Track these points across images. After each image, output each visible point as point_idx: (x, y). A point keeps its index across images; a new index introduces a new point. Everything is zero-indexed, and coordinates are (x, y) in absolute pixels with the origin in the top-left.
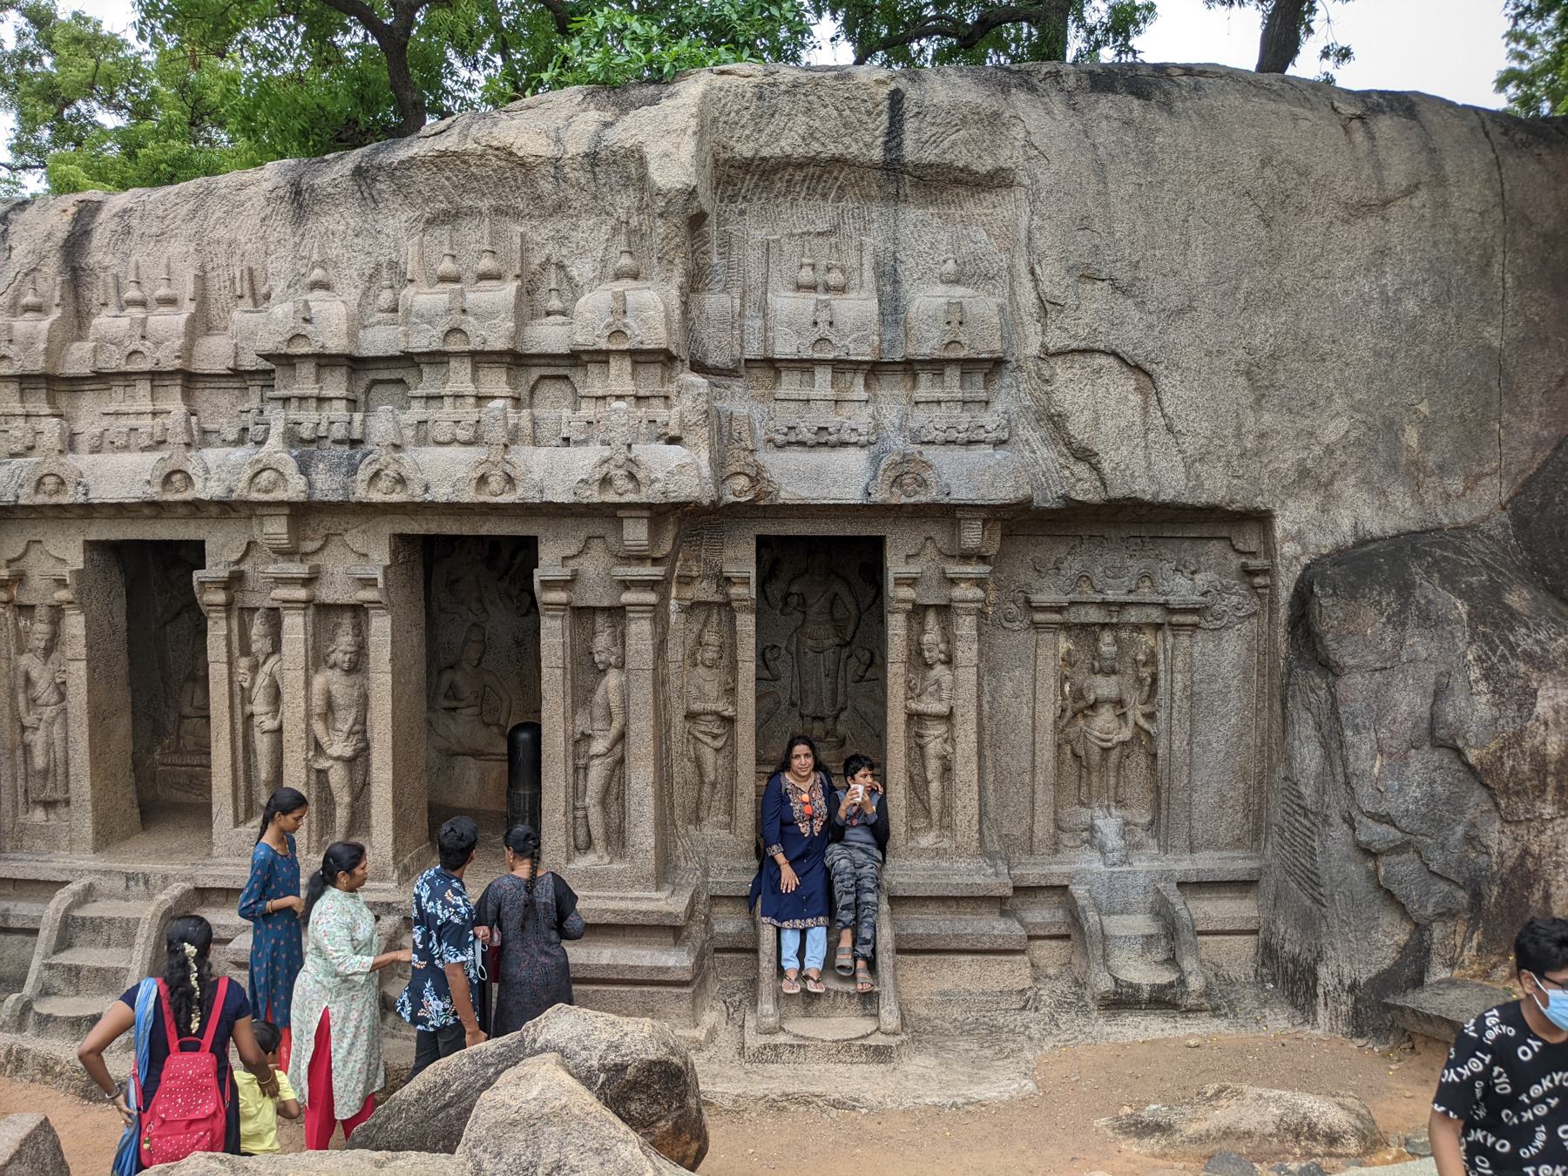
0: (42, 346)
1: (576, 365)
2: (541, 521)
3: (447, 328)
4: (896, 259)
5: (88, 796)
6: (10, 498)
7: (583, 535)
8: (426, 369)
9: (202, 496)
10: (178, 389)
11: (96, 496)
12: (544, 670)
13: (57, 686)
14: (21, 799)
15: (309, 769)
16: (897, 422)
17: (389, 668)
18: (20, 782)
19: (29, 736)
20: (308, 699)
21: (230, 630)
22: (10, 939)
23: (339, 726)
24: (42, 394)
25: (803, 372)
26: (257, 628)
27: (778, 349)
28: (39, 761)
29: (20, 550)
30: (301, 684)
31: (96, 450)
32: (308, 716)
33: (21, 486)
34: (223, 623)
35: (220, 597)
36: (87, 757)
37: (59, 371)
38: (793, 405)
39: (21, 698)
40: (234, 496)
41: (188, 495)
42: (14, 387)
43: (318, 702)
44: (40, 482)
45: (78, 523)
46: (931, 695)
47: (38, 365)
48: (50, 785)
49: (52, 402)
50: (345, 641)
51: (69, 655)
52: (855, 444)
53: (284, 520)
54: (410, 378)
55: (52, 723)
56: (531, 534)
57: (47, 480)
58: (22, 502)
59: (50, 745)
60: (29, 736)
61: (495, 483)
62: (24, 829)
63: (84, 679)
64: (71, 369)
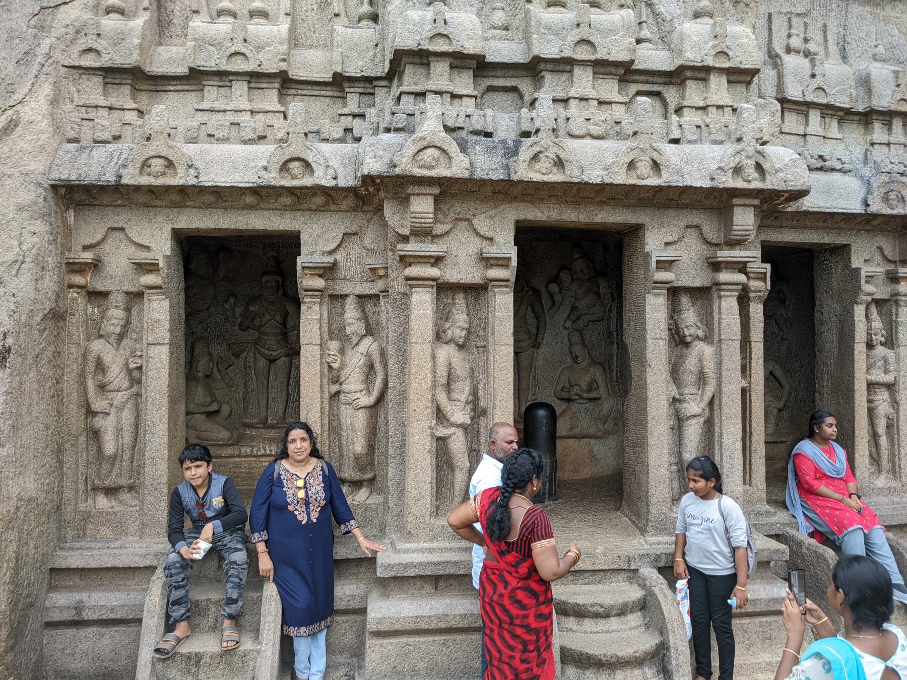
0: (136, 41)
1: (670, 83)
2: (648, 211)
3: (577, 38)
4: (845, 40)
5: (165, 479)
6: (111, 178)
7: (683, 224)
8: (548, 76)
9: (324, 183)
10: (275, 92)
11: (209, 179)
12: (649, 341)
13: (129, 372)
14: (81, 487)
15: (433, 435)
16: (861, 157)
17: (511, 341)
18: (81, 468)
19: (99, 422)
20: (434, 370)
21: (322, 316)
22: (83, 632)
23: (455, 395)
24: (126, 90)
25: (799, 112)
26: (351, 312)
27: (790, 92)
28: (109, 447)
29: (99, 237)
30: (429, 356)
31: (194, 140)
32: (434, 387)
33: (125, 166)
34: (316, 308)
35: (319, 283)
36: (165, 439)
37: (147, 69)
38: (793, 138)
39: (91, 384)
40: (398, 171)
41: (307, 181)
42: (97, 80)
43: (442, 373)
44: (145, 164)
45: (166, 211)
46: (880, 368)
47: (130, 59)
48: (114, 473)
49: (134, 98)
50: (460, 317)
51: (151, 340)
52: (840, 170)
53: (431, 200)
54: (525, 86)
55: (121, 409)
56: (640, 221)
57: (154, 162)
58: (125, 181)
59: (119, 430)
60: (99, 422)
61: (644, 167)
62: (87, 517)
63: (166, 363)
64: (157, 68)
